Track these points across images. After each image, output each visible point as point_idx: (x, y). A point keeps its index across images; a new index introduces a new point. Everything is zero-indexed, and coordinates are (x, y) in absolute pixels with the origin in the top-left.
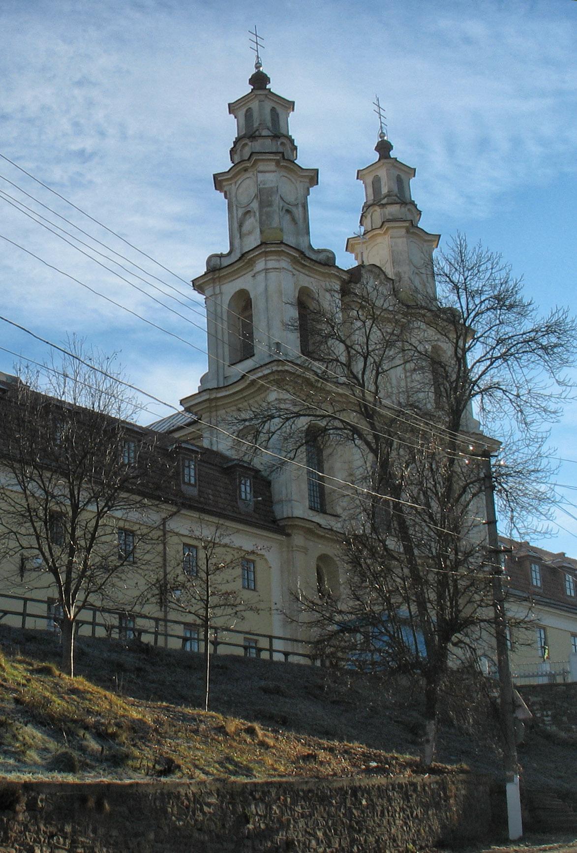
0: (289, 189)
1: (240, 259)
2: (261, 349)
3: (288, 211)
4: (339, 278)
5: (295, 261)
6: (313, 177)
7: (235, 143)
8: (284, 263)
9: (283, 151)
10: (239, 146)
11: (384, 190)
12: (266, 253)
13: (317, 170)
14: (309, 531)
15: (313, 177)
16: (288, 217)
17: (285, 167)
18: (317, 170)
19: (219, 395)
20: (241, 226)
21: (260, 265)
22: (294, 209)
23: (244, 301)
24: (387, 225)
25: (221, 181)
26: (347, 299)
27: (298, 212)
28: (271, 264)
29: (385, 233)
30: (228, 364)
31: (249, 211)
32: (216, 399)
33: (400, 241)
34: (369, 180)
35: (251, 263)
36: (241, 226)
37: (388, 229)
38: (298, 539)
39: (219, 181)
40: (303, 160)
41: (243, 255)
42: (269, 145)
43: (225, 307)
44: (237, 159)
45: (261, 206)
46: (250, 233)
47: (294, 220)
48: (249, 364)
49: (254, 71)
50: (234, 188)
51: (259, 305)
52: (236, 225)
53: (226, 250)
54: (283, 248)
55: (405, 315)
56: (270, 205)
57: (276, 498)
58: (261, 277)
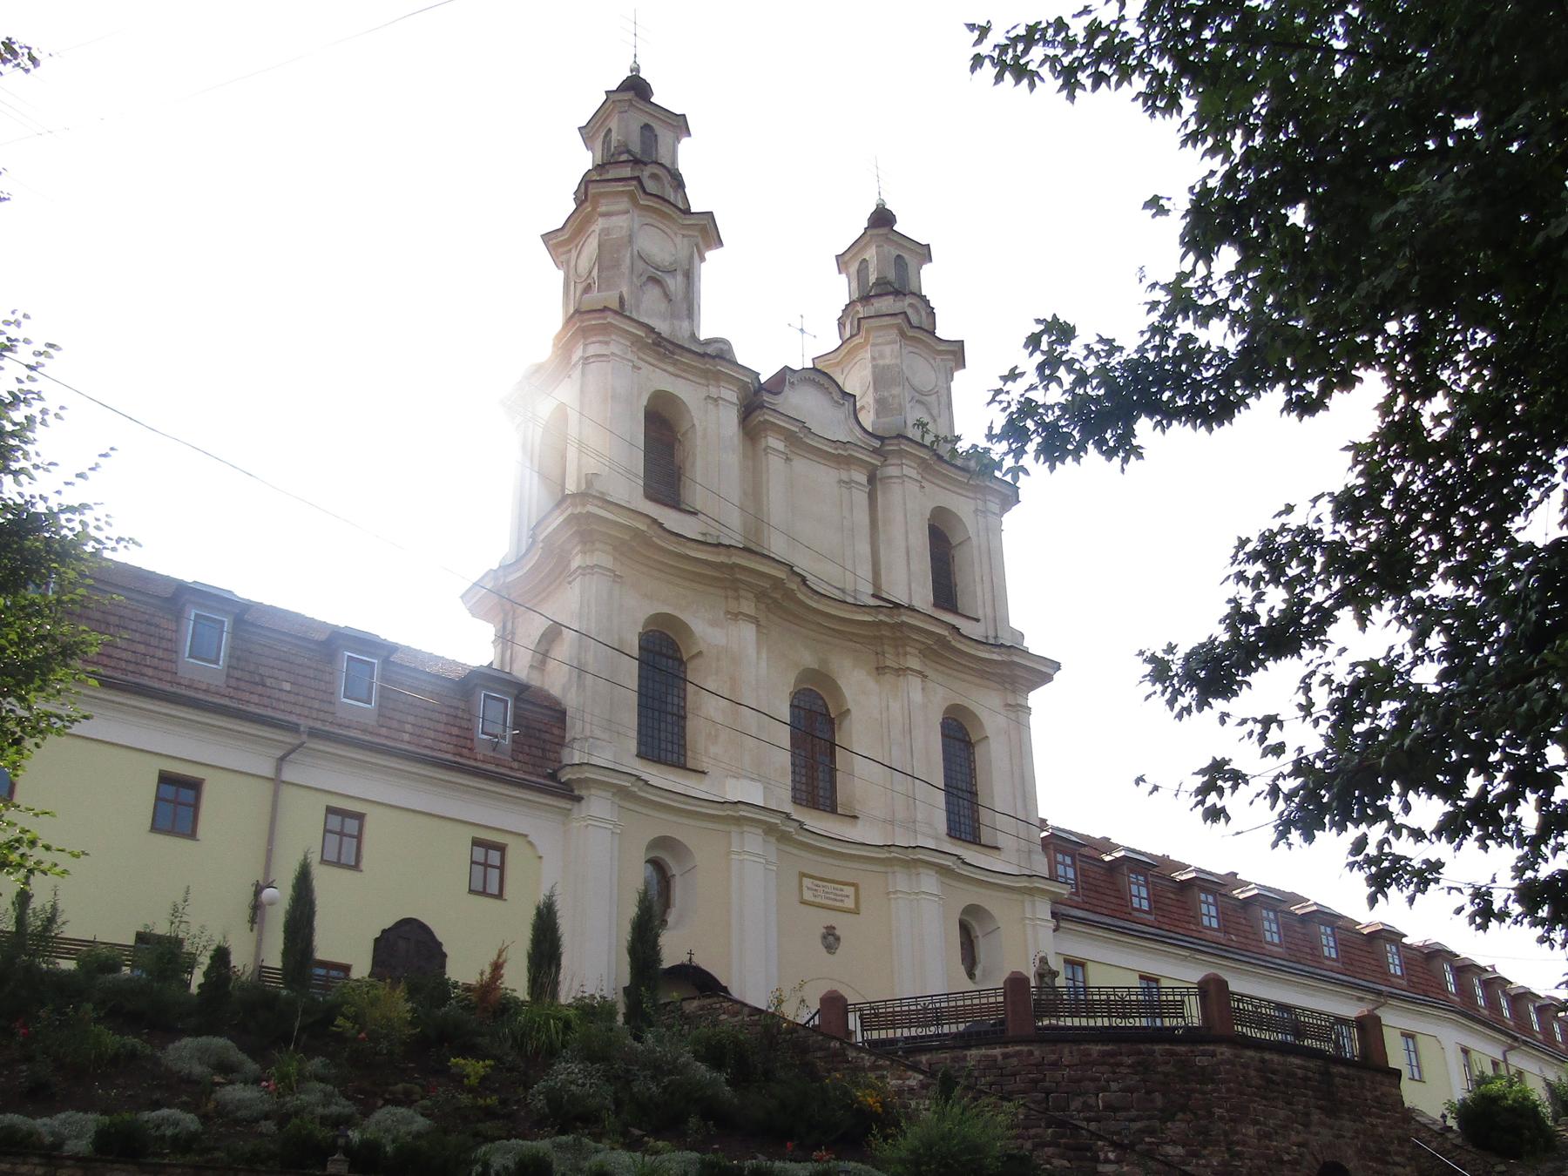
33: (887, 350)
38: (598, 806)
55: (875, 451)
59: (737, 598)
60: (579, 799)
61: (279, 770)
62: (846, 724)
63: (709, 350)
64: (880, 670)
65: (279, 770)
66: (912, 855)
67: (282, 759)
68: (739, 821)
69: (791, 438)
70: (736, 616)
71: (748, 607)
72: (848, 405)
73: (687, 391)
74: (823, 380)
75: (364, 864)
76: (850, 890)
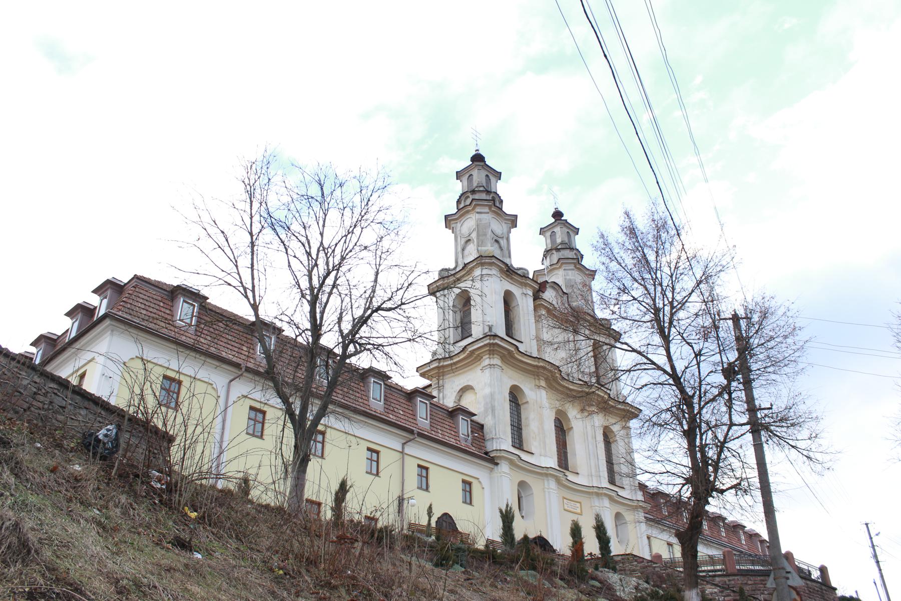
0: (498, 227)
1: (463, 268)
2: (477, 331)
3: (496, 241)
4: (531, 286)
5: (501, 270)
6: (513, 221)
7: (460, 197)
8: (494, 271)
9: (495, 203)
10: (463, 198)
11: (559, 241)
12: (482, 264)
13: (516, 216)
14: (511, 462)
15: (513, 221)
16: (496, 245)
17: (494, 212)
18: (516, 216)
19: (446, 363)
20: (463, 250)
21: (477, 272)
22: (501, 241)
23: (465, 300)
24: (561, 261)
26: (538, 302)
27: (503, 242)
28: (485, 272)
29: (560, 267)
31: (469, 240)
32: (443, 367)
33: (570, 272)
34: (548, 234)
36: (463, 250)
37: (562, 264)
38: (504, 467)
39: (449, 221)
40: (507, 208)
41: (465, 265)
42: (484, 196)
45: (478, 235)
47: (500, 247)
48: (469, 340)
49: (474, 153)
50: (459, 225)
51: (475, 299)
52: (460, 249)
53: (452, 266)
54: (494, 260)
56: (485, 235)
57: (487, 437)
59: (539, 379)
60: (497, 464)
61: (403, 448)
62: (571, 433)
63: (519, 272)
64: (583, 410)
65: (403, 448)
66: (601, 491)
67: (404, 444)
68: (547, 475)
69: (549, 311)
70: (539, 387)
71: (543, 383)
72: (565, 297)
73: (516, 290)
74: (556, 287)
75: (430, 489)
76: (578, 505)
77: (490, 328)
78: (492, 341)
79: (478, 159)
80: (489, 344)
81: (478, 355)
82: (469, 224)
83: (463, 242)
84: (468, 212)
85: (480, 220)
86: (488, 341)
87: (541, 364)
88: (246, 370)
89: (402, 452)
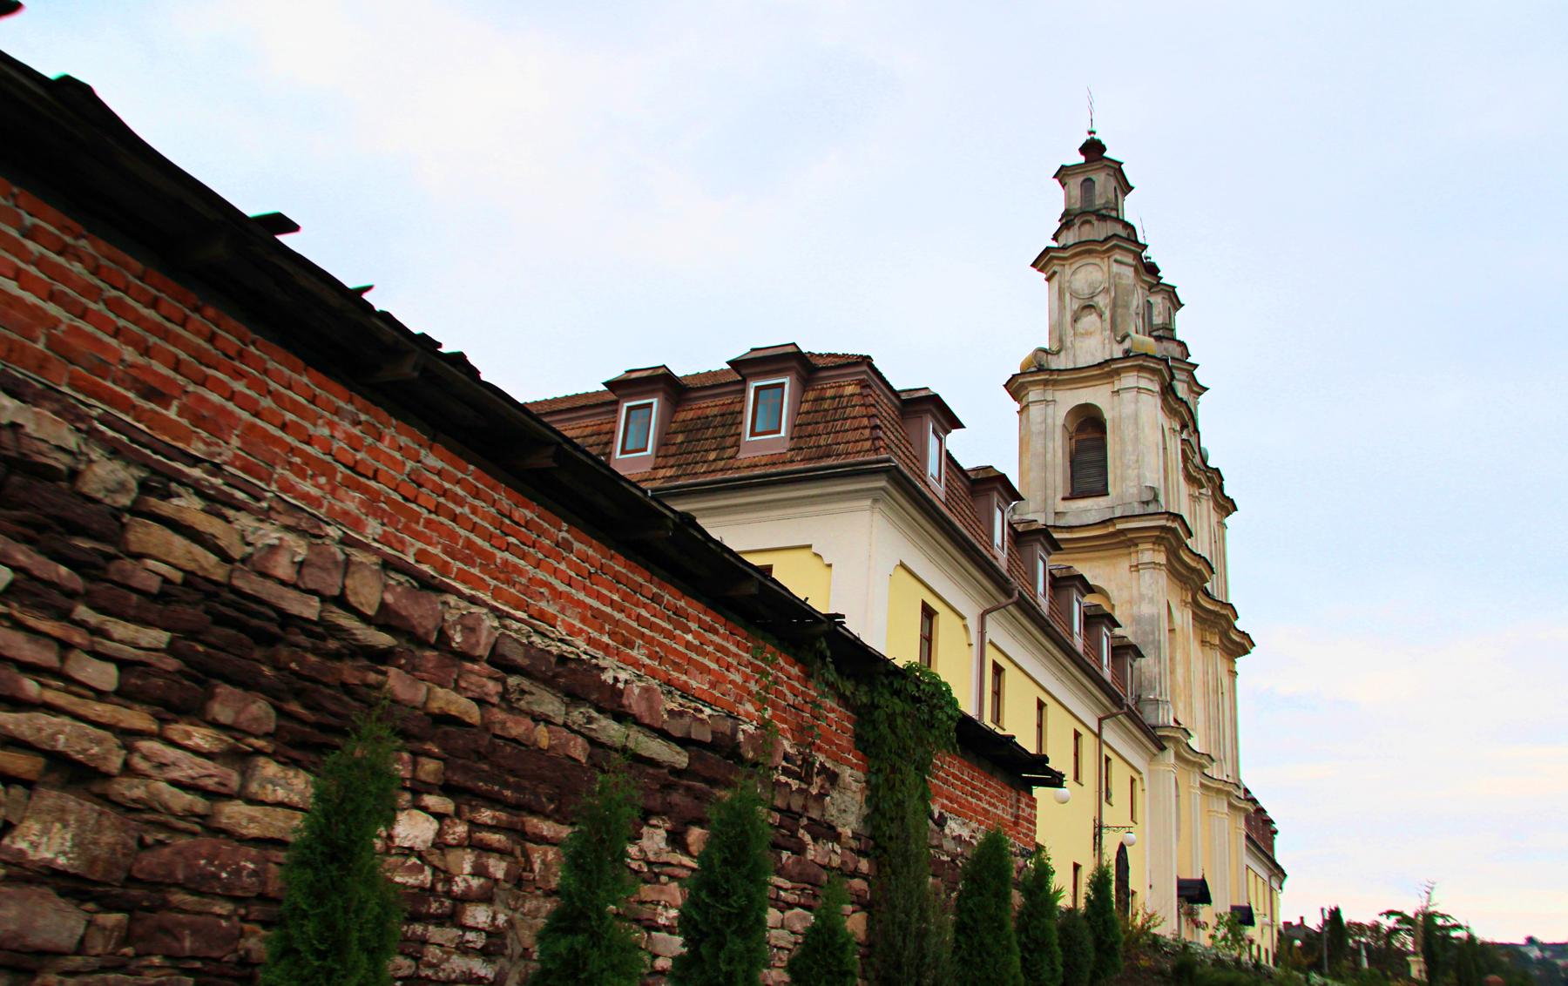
12: (1141, 368)
20: (1075, 320)
21: (1129, 380)
25: (1052, 258)
28: (1143, 383)
30: (1059, 496)
35: (1117, 372)
36: (1075, 320)
38: (1170, 756)
43: (1060, 421)
44: (1070, 238)
45: (1114, 306)
46: (1087, 334)
50: (1068, 270)
56: (1127, 307)
58: (1126, 396)
64: (1203, 642)
77: (1156, 499)
78: (1169, 524)
79: (1093, 149)
80: (1162, 528)
81: (1131, 540)
82: (1088, 275)
83: (1075, 307)
84: (1089, 252)
85: (1119, 275)
86: (1162, 523)
87: (1200, 567)
88: (1017, 604)
89: (1099, 735)
